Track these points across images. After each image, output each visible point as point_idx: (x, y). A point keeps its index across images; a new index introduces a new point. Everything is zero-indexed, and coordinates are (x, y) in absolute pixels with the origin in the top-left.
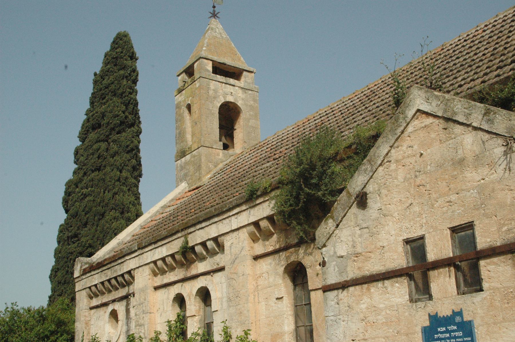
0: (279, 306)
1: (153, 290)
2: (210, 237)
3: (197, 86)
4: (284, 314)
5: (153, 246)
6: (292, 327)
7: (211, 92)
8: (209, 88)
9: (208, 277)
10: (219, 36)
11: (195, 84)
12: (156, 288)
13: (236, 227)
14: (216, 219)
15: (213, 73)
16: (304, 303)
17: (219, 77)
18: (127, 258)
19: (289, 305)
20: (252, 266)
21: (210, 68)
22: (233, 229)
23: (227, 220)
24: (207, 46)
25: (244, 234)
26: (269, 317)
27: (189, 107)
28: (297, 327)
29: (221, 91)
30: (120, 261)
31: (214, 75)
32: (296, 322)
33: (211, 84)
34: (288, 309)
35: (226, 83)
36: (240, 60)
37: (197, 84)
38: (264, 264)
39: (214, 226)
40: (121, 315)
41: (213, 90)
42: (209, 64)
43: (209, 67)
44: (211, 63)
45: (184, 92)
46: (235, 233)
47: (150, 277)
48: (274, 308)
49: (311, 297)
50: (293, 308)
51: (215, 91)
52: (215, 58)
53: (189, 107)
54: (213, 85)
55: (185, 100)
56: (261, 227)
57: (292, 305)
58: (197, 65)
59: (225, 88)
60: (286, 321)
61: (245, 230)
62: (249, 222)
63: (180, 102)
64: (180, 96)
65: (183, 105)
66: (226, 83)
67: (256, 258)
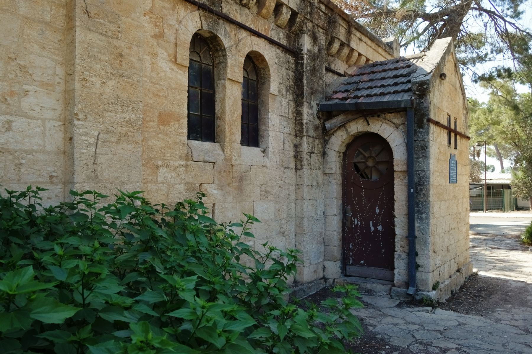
26: (157, 84)
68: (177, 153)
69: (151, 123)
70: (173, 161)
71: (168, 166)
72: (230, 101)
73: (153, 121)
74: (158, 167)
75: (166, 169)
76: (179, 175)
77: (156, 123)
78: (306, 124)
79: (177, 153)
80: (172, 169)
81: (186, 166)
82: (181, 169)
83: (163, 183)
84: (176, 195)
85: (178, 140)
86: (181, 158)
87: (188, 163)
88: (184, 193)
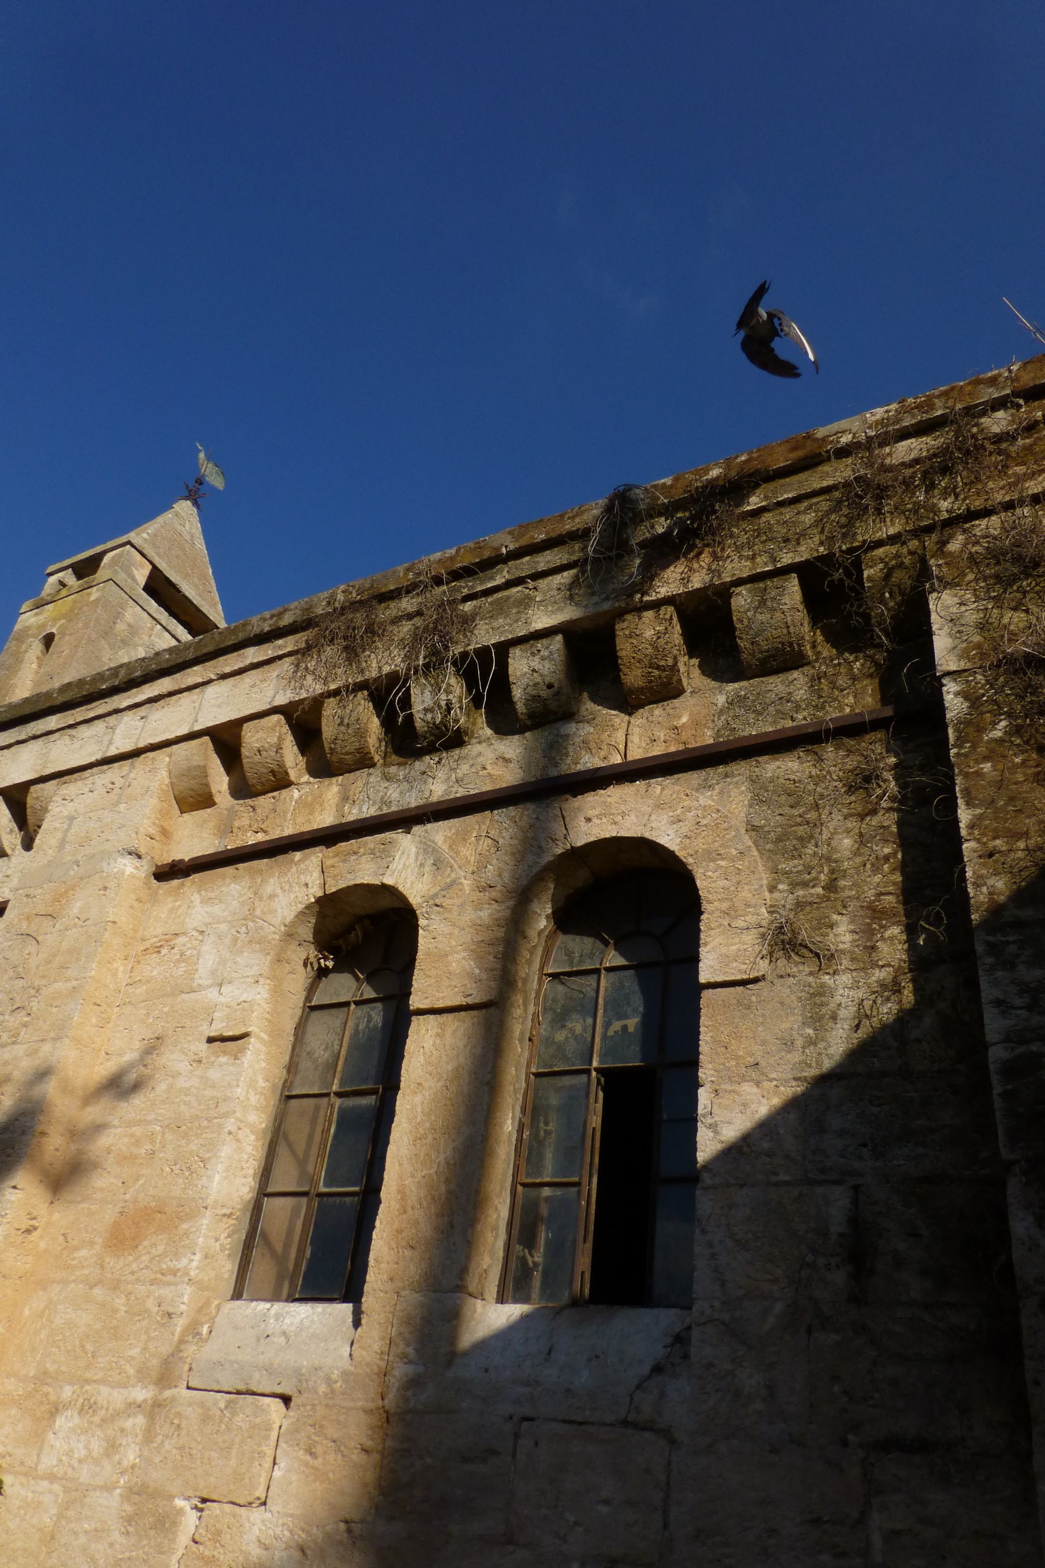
0: (214, 1074)
3: (92, 598)
4: (226, 1115)
6: (245, 1187)
7: (120, 627)
8: (118, 616)
10: (188, 538)
11: (89, 594)
13: (127, 747)
14: (52, 722)
15: (144, 589)
16: (335, 1088)
17: (153, 605)
19: (262, 1083)
20: (139, 900)
21: (142, 580)
22: (113, 751)
23: (99, 726)
24: (155, 535)
25: (155, 776)
26: (138, 1123)
27: (49, 640)
28: (263, 1193)
29: (146, 638)
31: (145, 595)
32: (266, 1173)
33: (130, 611)
34: (254, 1099)
35: (164, 628)
36: (214, 605)
37: (94, 594)
38: (196, 898)
39: (33, 745)
41: (129, 625)
42: (142, 566)
43: (142, 574)
44: (148, 569)
46: (114, 773)
48: (182, 1083)
49: (410, 1045)
50: (274, 1101)
51: (133, 630)
52: (163, 566)
53: (49, 640)
54: (132, 613)
55: (44, 626)
56: (245, 752)
57: (274, 1087)
59: (160, 637)
60: (226, 1151)
61: (162, 757)
62: (198, 727)
63: (29, 628)
64: (36, 614)
65: (35, 636)
66: (164, 628)
67: (169, 872)
68: (135, 1352)
69: (83, 1253)
70: (113, 1385)
71: (88, 1408)
72: (418, 1099)
73: (92, 1244)
74: (55, 1410)
75: (77, 1420)
76: (112, 1447)
77: (98, 1248)
78: (1009, 1070)
79: (135, 1352)
80: (96, 1419)
81: (155, 1409)
82: (128, 1424)
83: (52, 1478)
84: (82, 1539)
85: (150, 1304)
86: (142, 1374)
87: (168, 1393)
88: (116, 1536)
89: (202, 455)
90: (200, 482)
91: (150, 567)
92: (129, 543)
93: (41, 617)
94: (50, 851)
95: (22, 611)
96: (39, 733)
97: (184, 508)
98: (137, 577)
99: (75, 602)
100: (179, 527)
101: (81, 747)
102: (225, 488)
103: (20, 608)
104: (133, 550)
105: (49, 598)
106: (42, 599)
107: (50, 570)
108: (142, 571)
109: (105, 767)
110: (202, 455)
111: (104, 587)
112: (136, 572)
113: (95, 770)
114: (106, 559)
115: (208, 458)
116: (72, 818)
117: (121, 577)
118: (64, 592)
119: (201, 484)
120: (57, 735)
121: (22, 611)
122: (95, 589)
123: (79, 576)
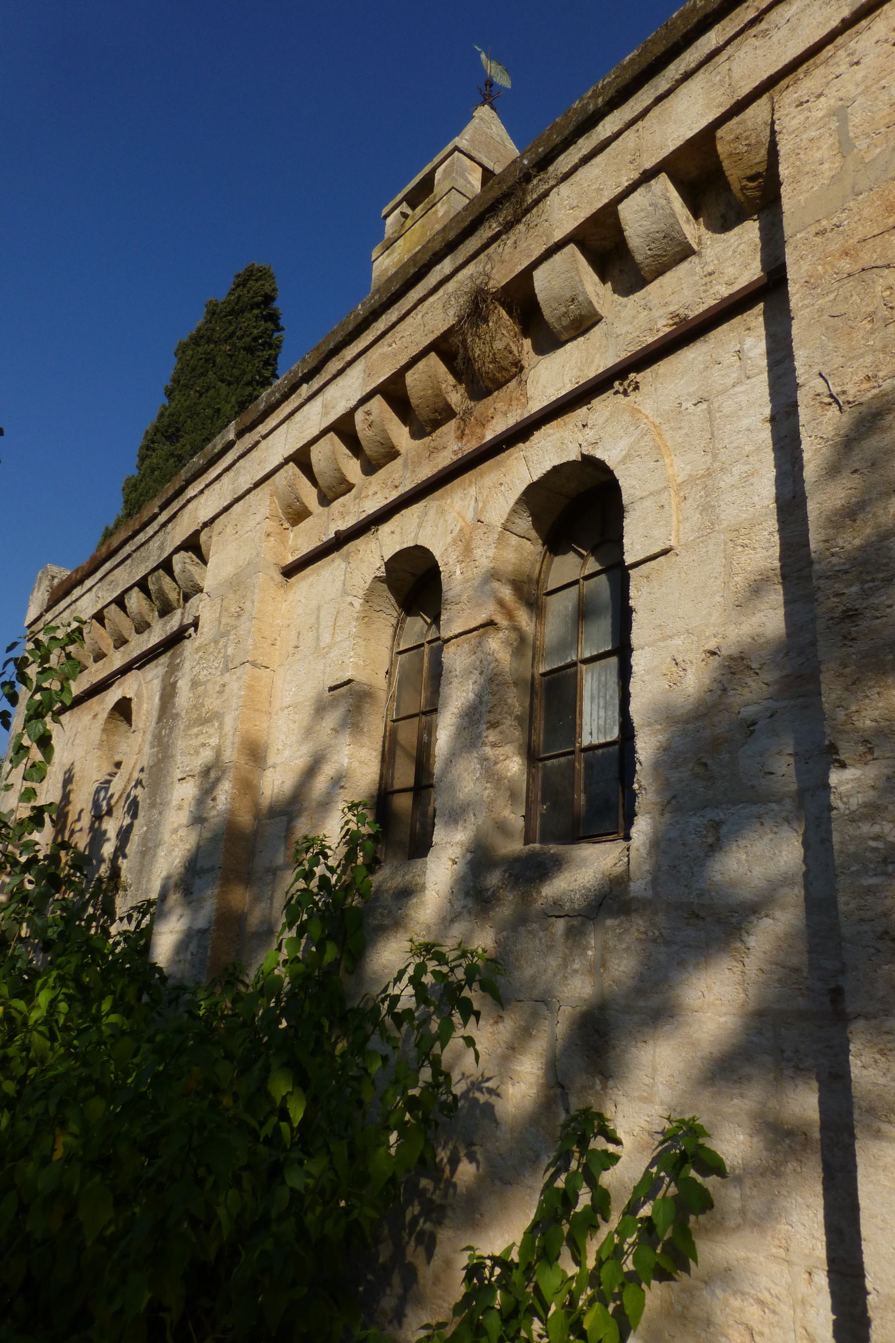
1: (279, 578)
2: (649, 163)
5: (305, 390)
9: (603, 407)
10: (498, 139)
11: (436, 211)
12: (290, 571)
14: (712, 39)
18: (191, 492)
30: (163, 518)
40: (145, 712)
42: (474, 171)
45: (400, 242)
47: (271, 525)
58: (445, 171)
64: (389, 255)
89: (483, 56)
90: (490, 83)
91: (481, 169)
92: (456, 149)
93: (395, 255)
94: (826, 166)
95: (373, 259)
96: (693, 65)
97: (484, 112)
98: (473, 182)
99: (423, 226)
100: (488, 131)
101: (793, 30)
102: (513, 85)
103: (371, 256)
104: (461, 155)
105: (396, 235)
106: (389, 238)
107: (384, 212)
108: (474, 175)
109: (864, 23)
110: (483, 56)
111: (448, 199)
112: (470, 178)
113: (840, 40)
114: (438, 175)
115: (490, 57)
116: (841, 113)
117: (460, 184)
118: (409, 222)
119: (491, 86)
120: (729, 50)
121: (373, 259)
122: (439, 204)
123: (413, 207)
